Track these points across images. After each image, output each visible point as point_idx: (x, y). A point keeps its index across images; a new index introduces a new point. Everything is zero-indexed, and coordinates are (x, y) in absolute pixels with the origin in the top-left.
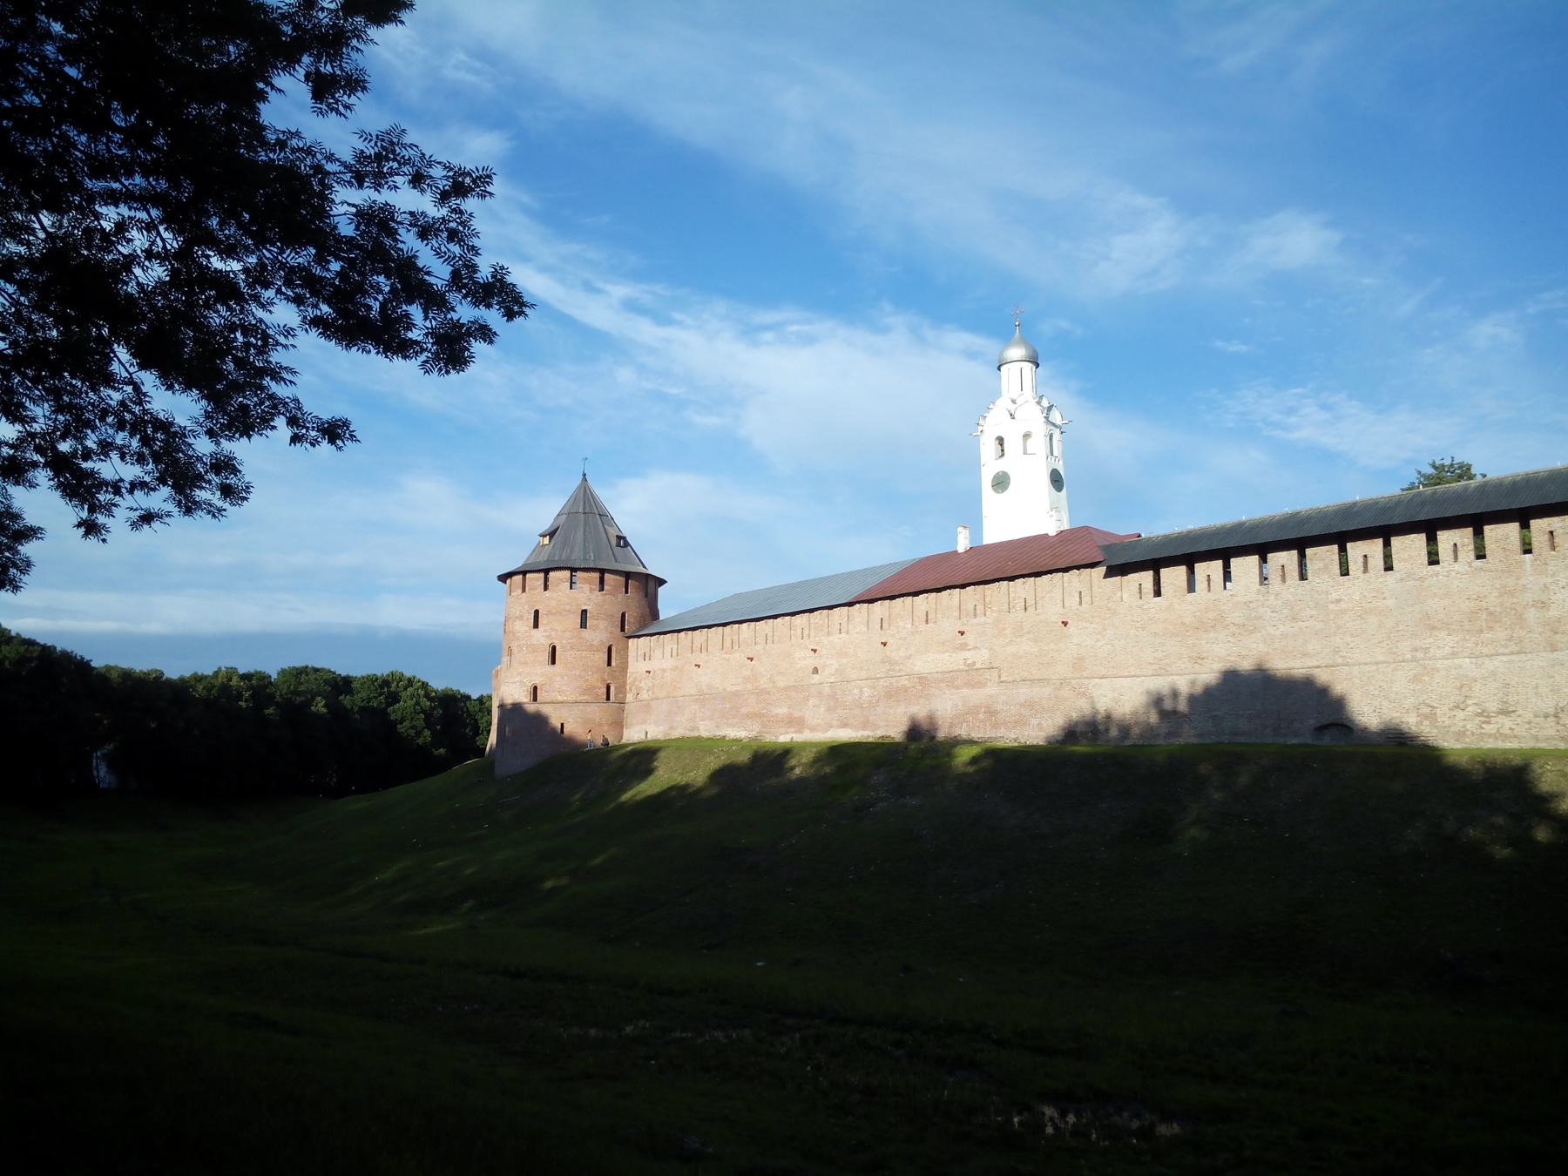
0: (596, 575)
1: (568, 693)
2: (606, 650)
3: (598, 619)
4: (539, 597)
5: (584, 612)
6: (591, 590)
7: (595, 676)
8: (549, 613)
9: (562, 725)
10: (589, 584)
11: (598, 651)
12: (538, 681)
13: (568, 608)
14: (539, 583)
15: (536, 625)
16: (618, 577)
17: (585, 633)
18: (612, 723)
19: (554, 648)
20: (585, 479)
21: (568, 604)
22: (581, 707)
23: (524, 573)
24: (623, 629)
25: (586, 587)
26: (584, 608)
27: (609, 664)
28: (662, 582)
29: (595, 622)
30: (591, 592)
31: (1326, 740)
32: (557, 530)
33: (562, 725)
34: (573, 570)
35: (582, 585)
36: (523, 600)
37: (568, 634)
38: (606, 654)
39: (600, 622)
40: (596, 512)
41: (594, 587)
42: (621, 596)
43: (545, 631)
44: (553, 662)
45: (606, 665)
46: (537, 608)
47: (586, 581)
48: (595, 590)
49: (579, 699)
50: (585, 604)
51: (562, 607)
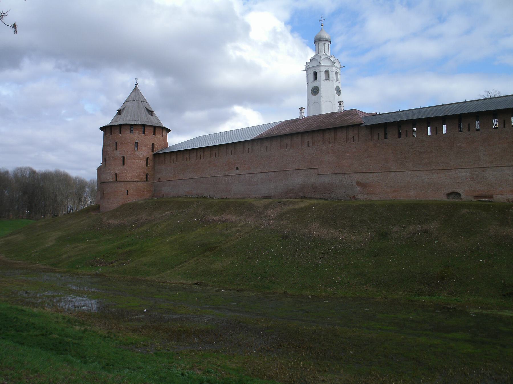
1: (130, 177)
2: (145, 159)
3: (142, 146)
4: (117, 137)
5: (137, 143)
6: (139, 133)
7: (141, 170)
11: (142, 160)
12: (117, 172)
13: (129, 141)
14: (117, 131)
15: (116, 149)
17: (137, 152)
18: (148, 191)
19: (124, 158)
20: (136, 87)
22: (135, 183)
24: (153, 150)
25: (137, 133)
26: (136, 141)
27: (147, 165)
28: (168, 131)
29: (141, 147)
30: (139, 135)
31: (452, 200)
35: (135, 132)
36: (111, 138)
38: (146, 161)
41: (140, 132)
42: (152, 136)
43: (120, 151)
44: (124, 164)
45: (145, 166)
46: (116, 141)
48: (141, 134)
49: (134, 180)
50: (137, 140)
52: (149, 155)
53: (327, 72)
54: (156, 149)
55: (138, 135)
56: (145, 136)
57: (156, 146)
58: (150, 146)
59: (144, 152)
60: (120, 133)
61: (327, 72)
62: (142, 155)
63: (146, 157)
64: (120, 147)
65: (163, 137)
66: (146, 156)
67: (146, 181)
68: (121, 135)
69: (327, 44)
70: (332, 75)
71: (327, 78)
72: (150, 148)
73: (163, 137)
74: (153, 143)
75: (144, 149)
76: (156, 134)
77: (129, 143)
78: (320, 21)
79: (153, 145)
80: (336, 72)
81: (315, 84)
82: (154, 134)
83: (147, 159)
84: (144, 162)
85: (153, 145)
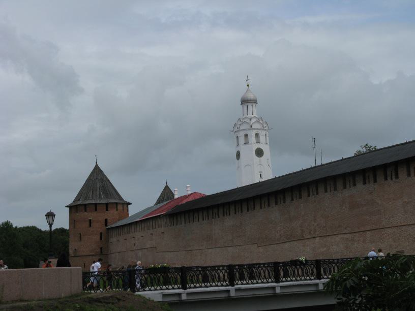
2: (99, 234)
5: (90, 220)
9: (84, 264)
12: (76, 248)
24: (106, 225)
27: (101, 239)
33: (84, 264)
53: (246, 136)
59: (98, 227)
61: (246, 136)
65: (117, 210)
67: (101, 252)
69: (254, 105)
70: (252, 139)
71: (247, 143)
72: (104, 223)
73: (117, 210)
79: (106, 220)
80: (257, 135)
81: (238, 149)
82: (107, 210)
83: (101, 234)
84: (97, 237)
85: (106, 220)
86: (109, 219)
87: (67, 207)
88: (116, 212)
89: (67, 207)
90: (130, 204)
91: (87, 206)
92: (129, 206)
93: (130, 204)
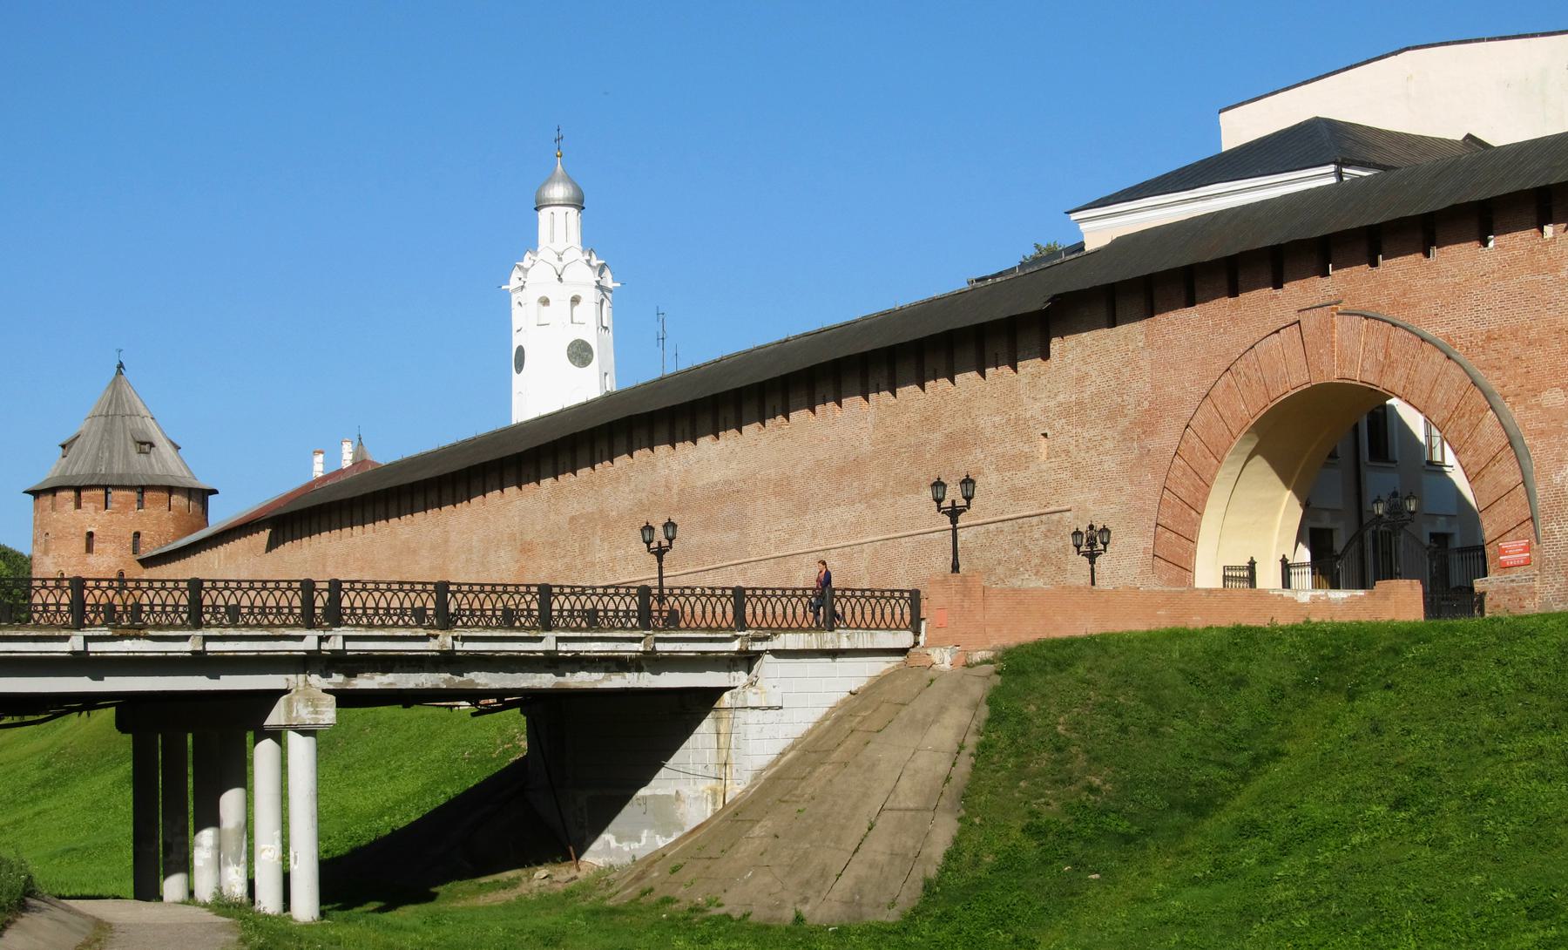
0: (102, 492)
5: (91, 535)
6: (96, 509)
8: (57, 538)
10: (94, 502)
13: (73, 530)
16: (127, 493)
21: (73, 526)
23: (53, 491)
24: (135, 551)
26: (89, 530)
30: (96, 512)
32: (78, 436)
34: (78, 490)
37: (73, 561)
39: (108, 544)
40: (143, 412)
41: (99, 506)
46: (47, 531)
47: (91, 499)
50: (90, 526)
51: (68, 530)
52: (125, 563)
54: (148, 546)
55: (94, 514)
56: (113, 513)
57: (144, 538)
58: (128, 539)
60: (53, 509)
62: (105, 566)
63: (117, 570)
64: (54, 547)
66: (117, 567)
68: (55, 515)
69: (573, 211)
72: (129, 544)
74: (136, 530)
75: (110, 547)
76: (147, 504)
77: (73, 537)
78: (556, 141)
79: (137, 535)
85: (137, 535)
86: (144, 533)
87: (25, 492)
88: (167, 515)
89: (25, 492)
90: (215, 492)
91: (83, 494)
92: (211, 498)
93: (215, 492)
